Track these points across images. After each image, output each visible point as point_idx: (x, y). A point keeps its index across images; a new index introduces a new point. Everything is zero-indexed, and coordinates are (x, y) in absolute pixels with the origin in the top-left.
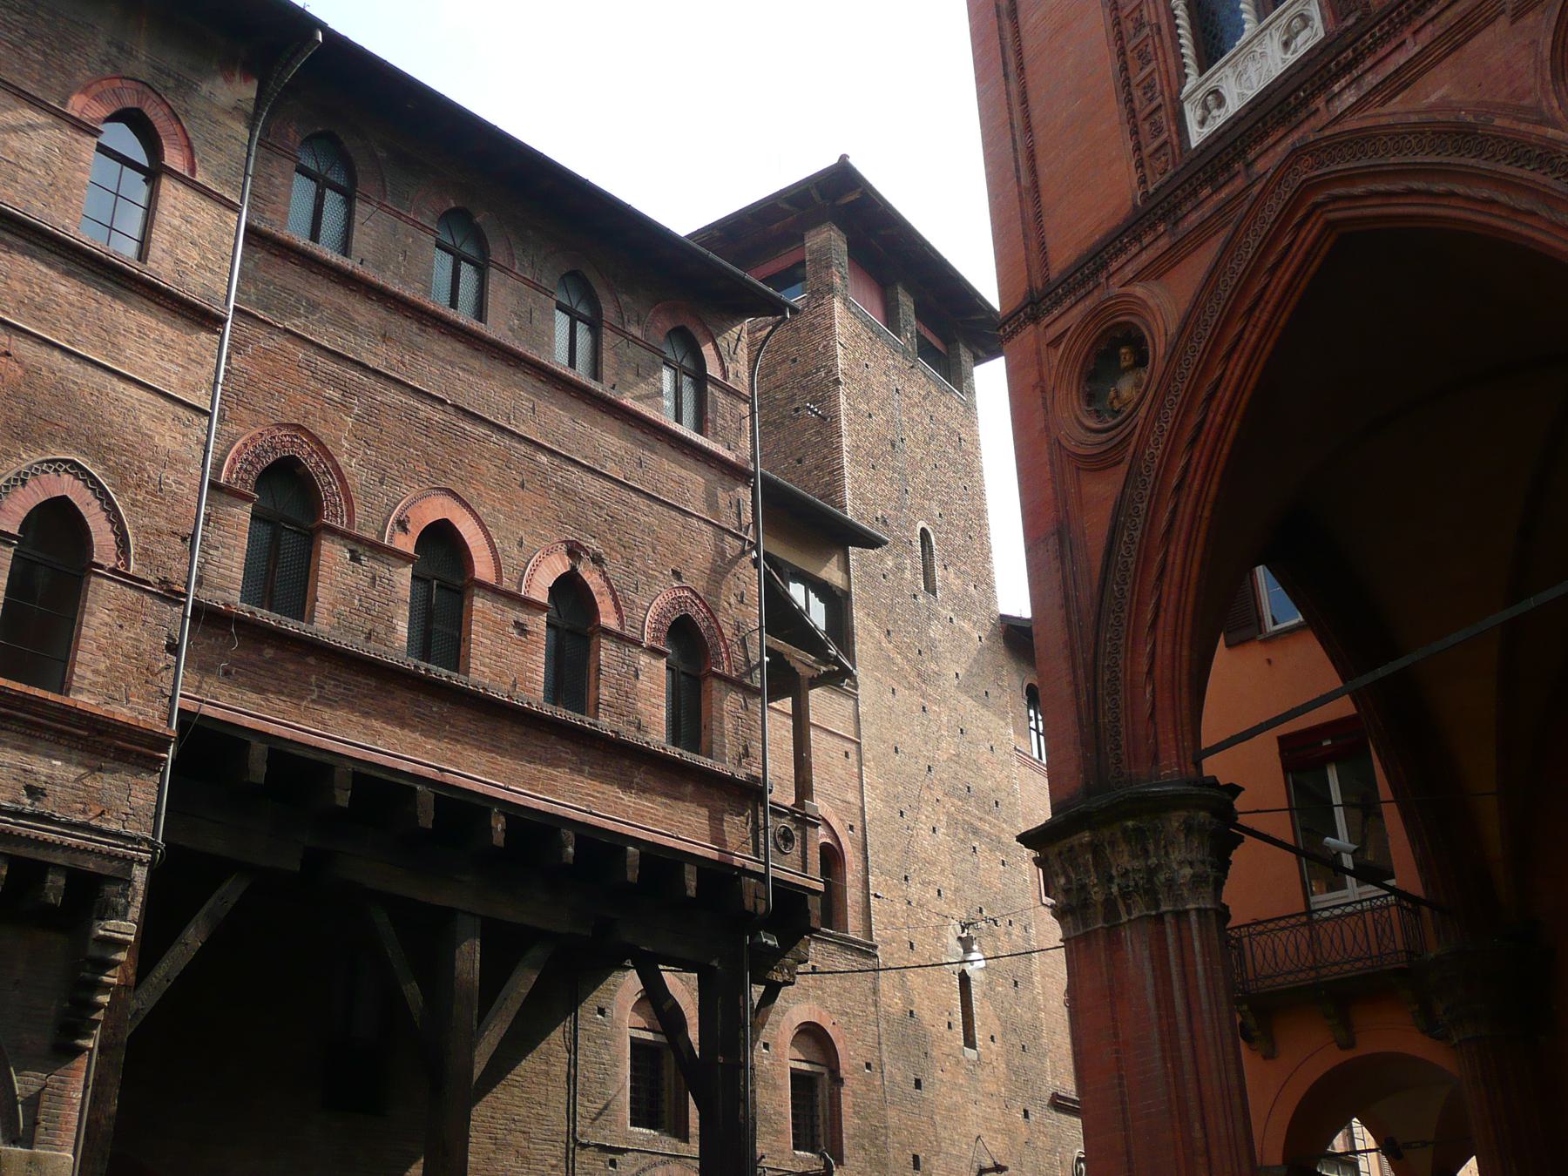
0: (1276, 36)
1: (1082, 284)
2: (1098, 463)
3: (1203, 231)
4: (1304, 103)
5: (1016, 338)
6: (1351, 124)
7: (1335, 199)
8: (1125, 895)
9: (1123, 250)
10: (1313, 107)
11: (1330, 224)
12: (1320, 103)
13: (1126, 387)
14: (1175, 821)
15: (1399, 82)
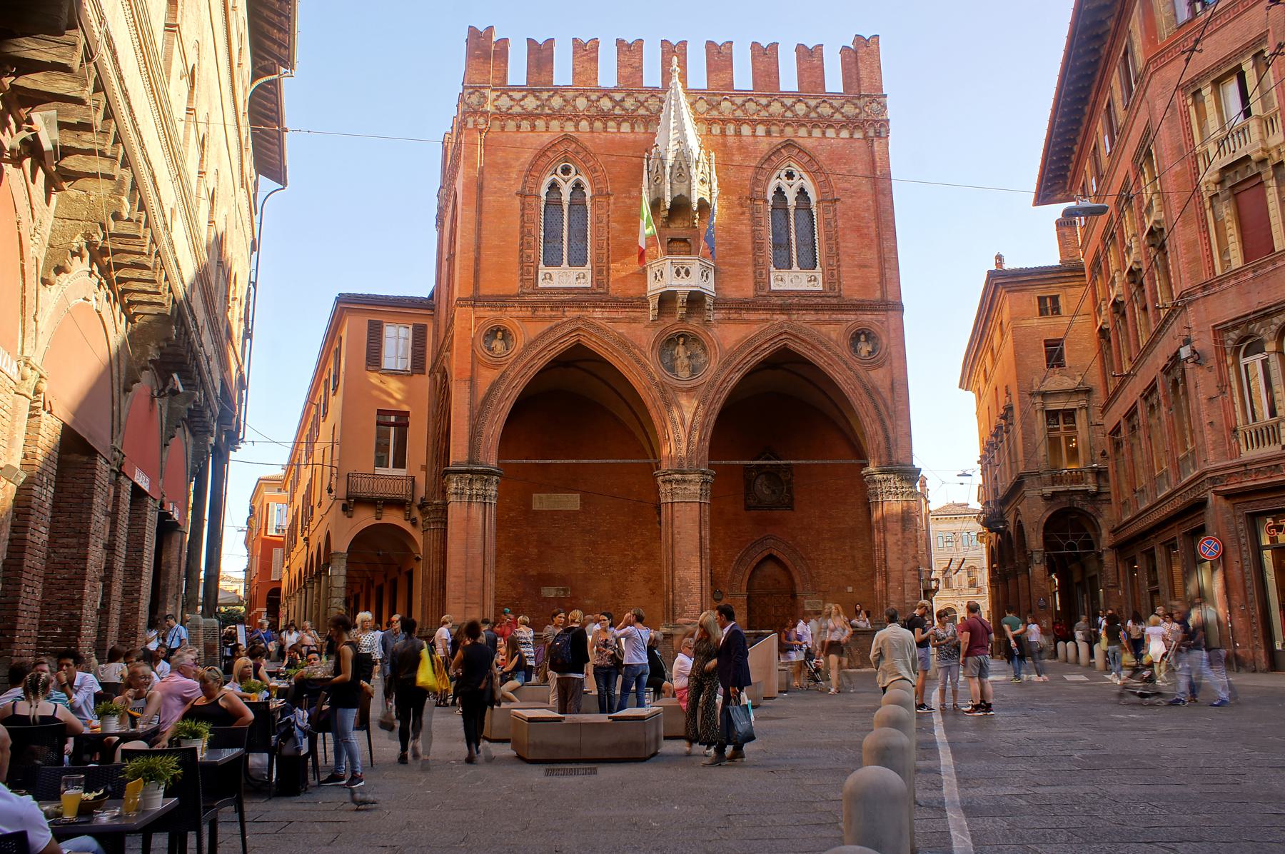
3: (543, 319)
6: (598, 322)
8: (477, 495)
10: (589, 309)
12: (591, 310)
13: (498, 345)
14: (495, 478)
15: (612, 320)
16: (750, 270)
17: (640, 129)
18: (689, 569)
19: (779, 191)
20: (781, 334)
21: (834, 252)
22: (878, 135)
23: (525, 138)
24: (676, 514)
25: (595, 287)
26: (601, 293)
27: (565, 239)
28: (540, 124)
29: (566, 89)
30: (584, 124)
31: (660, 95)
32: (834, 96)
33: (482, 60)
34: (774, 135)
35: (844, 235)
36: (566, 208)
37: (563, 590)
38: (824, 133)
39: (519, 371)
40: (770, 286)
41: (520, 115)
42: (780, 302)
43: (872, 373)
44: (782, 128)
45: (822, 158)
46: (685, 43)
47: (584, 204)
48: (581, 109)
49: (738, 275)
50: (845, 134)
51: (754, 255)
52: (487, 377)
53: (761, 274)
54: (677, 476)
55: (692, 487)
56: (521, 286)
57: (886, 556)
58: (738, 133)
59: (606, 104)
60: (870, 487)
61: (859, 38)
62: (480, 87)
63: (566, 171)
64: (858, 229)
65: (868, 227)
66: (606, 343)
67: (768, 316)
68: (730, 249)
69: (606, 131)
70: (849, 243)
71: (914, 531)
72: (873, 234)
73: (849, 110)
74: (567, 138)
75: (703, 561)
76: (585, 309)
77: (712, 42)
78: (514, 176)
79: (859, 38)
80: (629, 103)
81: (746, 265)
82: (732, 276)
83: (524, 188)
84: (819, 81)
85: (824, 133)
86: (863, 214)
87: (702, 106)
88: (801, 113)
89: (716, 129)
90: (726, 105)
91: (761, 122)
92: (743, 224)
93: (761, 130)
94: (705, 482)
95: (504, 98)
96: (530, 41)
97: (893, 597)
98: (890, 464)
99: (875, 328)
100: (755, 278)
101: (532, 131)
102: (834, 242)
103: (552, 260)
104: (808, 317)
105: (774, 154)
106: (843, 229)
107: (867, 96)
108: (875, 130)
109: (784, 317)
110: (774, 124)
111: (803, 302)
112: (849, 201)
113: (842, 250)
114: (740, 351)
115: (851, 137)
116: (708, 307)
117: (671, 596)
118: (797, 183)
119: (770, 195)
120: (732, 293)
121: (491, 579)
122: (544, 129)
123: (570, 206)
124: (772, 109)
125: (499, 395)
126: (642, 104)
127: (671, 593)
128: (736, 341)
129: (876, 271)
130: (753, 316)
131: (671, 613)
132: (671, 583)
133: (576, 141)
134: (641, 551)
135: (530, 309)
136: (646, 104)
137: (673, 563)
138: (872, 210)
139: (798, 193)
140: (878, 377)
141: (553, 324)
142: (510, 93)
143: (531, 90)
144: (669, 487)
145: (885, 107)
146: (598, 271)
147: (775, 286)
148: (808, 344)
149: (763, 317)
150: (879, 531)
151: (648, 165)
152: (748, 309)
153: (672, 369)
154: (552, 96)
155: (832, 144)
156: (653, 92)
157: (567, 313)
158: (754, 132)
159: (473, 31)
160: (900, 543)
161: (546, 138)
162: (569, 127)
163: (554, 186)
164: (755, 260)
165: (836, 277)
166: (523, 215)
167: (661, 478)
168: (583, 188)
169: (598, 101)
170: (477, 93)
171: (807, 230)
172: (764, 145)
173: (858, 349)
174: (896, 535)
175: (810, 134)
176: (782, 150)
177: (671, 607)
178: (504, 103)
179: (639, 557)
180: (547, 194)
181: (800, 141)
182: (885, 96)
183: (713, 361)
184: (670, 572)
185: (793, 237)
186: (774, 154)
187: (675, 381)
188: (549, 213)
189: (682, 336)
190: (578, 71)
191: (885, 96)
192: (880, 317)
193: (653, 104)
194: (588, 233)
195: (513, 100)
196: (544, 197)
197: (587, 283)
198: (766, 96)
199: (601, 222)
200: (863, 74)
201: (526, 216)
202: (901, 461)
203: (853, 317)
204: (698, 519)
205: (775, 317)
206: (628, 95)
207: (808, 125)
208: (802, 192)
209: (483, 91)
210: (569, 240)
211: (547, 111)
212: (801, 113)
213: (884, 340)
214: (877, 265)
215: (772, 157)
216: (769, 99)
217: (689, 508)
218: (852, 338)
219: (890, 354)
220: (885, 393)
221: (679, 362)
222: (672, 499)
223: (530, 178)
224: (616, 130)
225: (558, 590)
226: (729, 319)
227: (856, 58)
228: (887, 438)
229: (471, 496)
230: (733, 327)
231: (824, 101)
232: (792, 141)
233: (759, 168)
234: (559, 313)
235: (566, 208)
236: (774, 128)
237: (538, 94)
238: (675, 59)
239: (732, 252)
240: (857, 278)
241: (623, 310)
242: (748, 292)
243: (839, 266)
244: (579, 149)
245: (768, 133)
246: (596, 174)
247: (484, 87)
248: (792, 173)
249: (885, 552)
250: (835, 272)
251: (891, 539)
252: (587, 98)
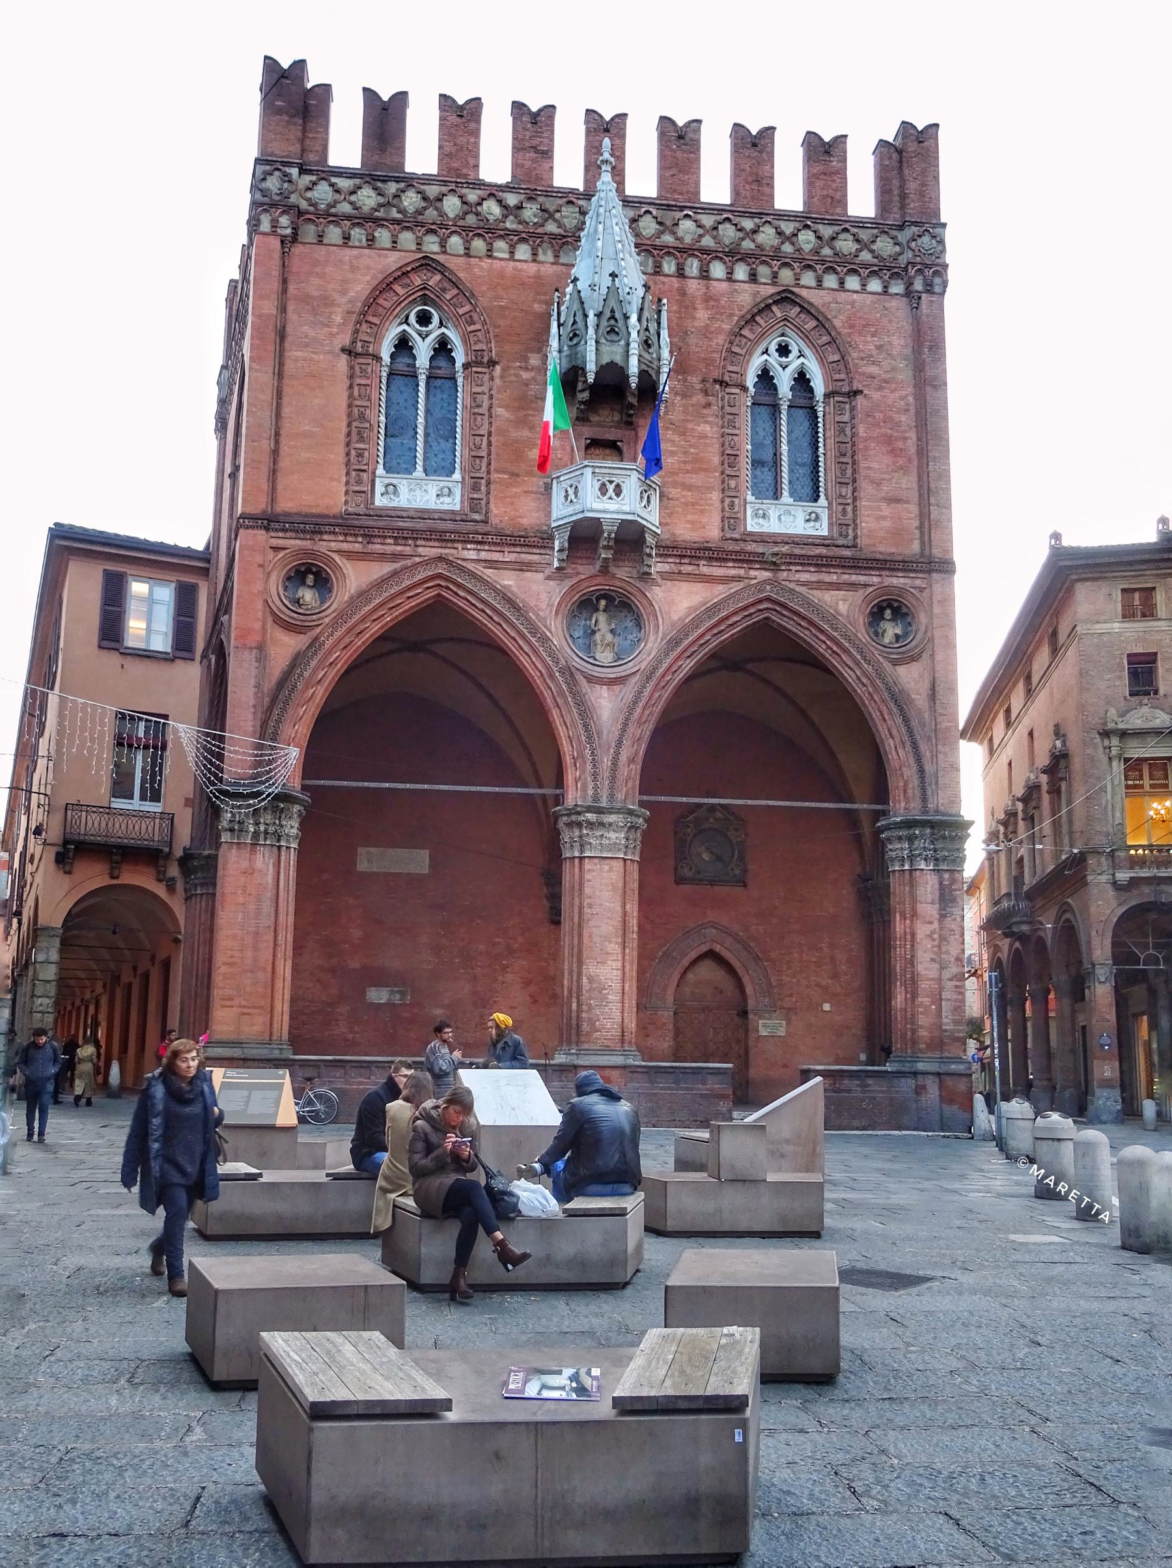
0: (435, 488)
1: (304, 532)
2: (290, 627)
3: (382, 557)
4: (453, 541)
5: (250, 531)
6: (470, 566)
7: (447, 588)
8: (266, 832)
9: (334, 533)
10: (456, 545)
11: (439, 595)
12: (459, 546)
14: (296, 808)
15: (491, 564)
16: (715, 496)
17: (546, 256)
18: (603, 963)
19: (766, 378)
20: (760, 601)
21: (849, 478)
22: (929, 288)
23: (357, 257)
24: (587, 876)
25: (467, 510)
26: (476, 521)
27: (420, 431)
28: (383, 236)
29: (427, 179)
30: (455, 242)
31: (581, 202)
32: (860, 223)
33: (286, 118)
34: (763, 280)
35: (866, 449)
36: (422, 379)
37: (398, 992)
38: (842, 283)
39: (341, 639)
40: (745, 525)
41: (348, 217)
42: (761, 550)
43: (902, 670)
44: (776, 269)
45: (837, 323)
46: (623, 116)
47: (453, 379)
48: (451, 215)
49: (697, 503)
50: (875, 285)
51: (723, 473)
52: (285, 645)
53: (732, 505)
54: (589, 816)
55: (613, 835)
56: (346, 502)
57: (913, 956)
58: (705, 275)
59: (492, 209)
60: (890, 847)
61: (906, 126)
62: (285, 164)
63: (424, 319)
64: (889, 440)
65: (906, 439)
66: (482, 601)
67: (742, 572)
68: (685, 462)
69: (490, 256)
70: (874, 462)
71: (959, 919)
72: (913, 450)
73: (885, 246)
74: (427, 263)
75: (627, 951)
76: (449, 545)
77: (669, 119)
78: (338, 319)
79: (906, 126)
80: (530, 212)
81: (710, 489)
82: (686, 504)
83: (354, 342)
84: (838, 196)
85: (842, 283)
86: (896, 417)
87: (648, 226)
88: (807, 248)
89: (669, 266)
90: (687, 226)
91: (744, 258)
92: (707, 422)
93: (741, 272)
94: (633, 828)
95: (323, 187)
96: (370, 95)
97: (923, 1020)
98: (925, 811)
99: (908, 601)
100: (723, 510)
101: (369, 247)
102: (850, 461)
103: (400, 464)
104: (805, 577)
105: (760, 312)
106: (866, 440)
107: (915, 223)
108: (925, 279)
109: (767, 575)
110: (763, 262)
111: (797, 551)
112: (876, 395)
113: (863, 472)
114: (696, 622)
115: (885, 292)
116: (648, 550)
117: (574, 1005)
118: (794, 363)
119: (751, 380)
120: (685, 532)
121: (285, 969)
122: (389, 245)
123: (429, 378)
124: (760, 238)
125: (306, 674)
126: (551, 216)
127: (574, 1000)
128: (689, 608)
129: (914, 509)
130: (718, 571)
131: (574, 1032)
132: (575, 983)
133: (440, 268)
134: (520, 939)
135: (360, 539)
136: (557, 215)
137: (580, 952)
138: (913, 411)
139: (795, 379)
140: (910, 677)
141: (397, 566)
142: (334, 180)
143: (369, 176)
144: (577, 833)
145: (941, 242)
146: (473, 484)
147: (753, 525)
148: (804, 618)
149: (733, 572)
150: (904, 917)
151: (559, 314)
152: (710, 559)
153: (589, 648)
154: (403, 191)
155: (854, 301)
156: (569, 196)
157: (420, 550)
158: (731, 273)
159: (270, 64)
160: (936, 936)
161: (393, 261)
162: (432, 245)
163: (403, 345)
164: (723, 482)
165: (850, 515)
166: (351, 387)
167: (565, 819)
168: (451, 350)
169: (480, 204)
170: (277, 173)
171: (805, 442)
172: (746, 296)
173: (880, 631)
174: (931, 923)
175: (819, 281)
176: (774, 308)
177: (574, 1022)
178: (323, 196)
179: (516, 946)
180: (392, 356)
181: (804, 293)
182: (944, 225)
183: (652, 638)
184: (575, 966)
185: (784, 448)
186: (760, 312)
187: (590, 667)
188: (393, 387)
189: (604, 596)
190: (447, 150)
191: (944, 225)
192: (918, 582)
193: (569, 216)
194: (459, 423)
195: (337, 191)
196: (386, 359)
197: (454, 503)
198: (752, 215)
199: (479, 406)
200: (912, 186)
201: (356, 389)
202: (942, 808)
203: (875, 579)
204: (621, 884)
205: (753, 573)
206: (530, 199)
207: (817, 267)
208: (802, 380)
209: (287, 170)
210: (427, 435)
211: (394, 214)
212: (807, 248)
213: (923, 618)
214: (916, 500)
215: (758, 318)
216: (757, 220)
217: (606, 868)
218: (872, 614)
219: (931, 640)
220: (920, 699)
221: (598, 637)
222: (582, 851)
223: (364, 326)
224: (506, 256)
225: (392, 992)
226: (680, 573)
227: (901, 162)
228: (921, 771)
229: (256, 834)
230: (685, 587)
231: (846, 230)
232: (792, 293)
233: (737, 334)
234: (408, 548)
235: (422, 379)
236: (764, 271)
237: (379, 184)
238: (607, 142)
239: (688, 467)
240: (884, 518)
241: (512, 549)
242: (712, 531)
243: (855, 499)
244: (446, 285)
245: (753, 277)
246: (472, 328)
247: (289, 164)
248: (787, 346)
249: (913, 946)
250: (849, 509)
251: (922, 930)
252: (461, 197)
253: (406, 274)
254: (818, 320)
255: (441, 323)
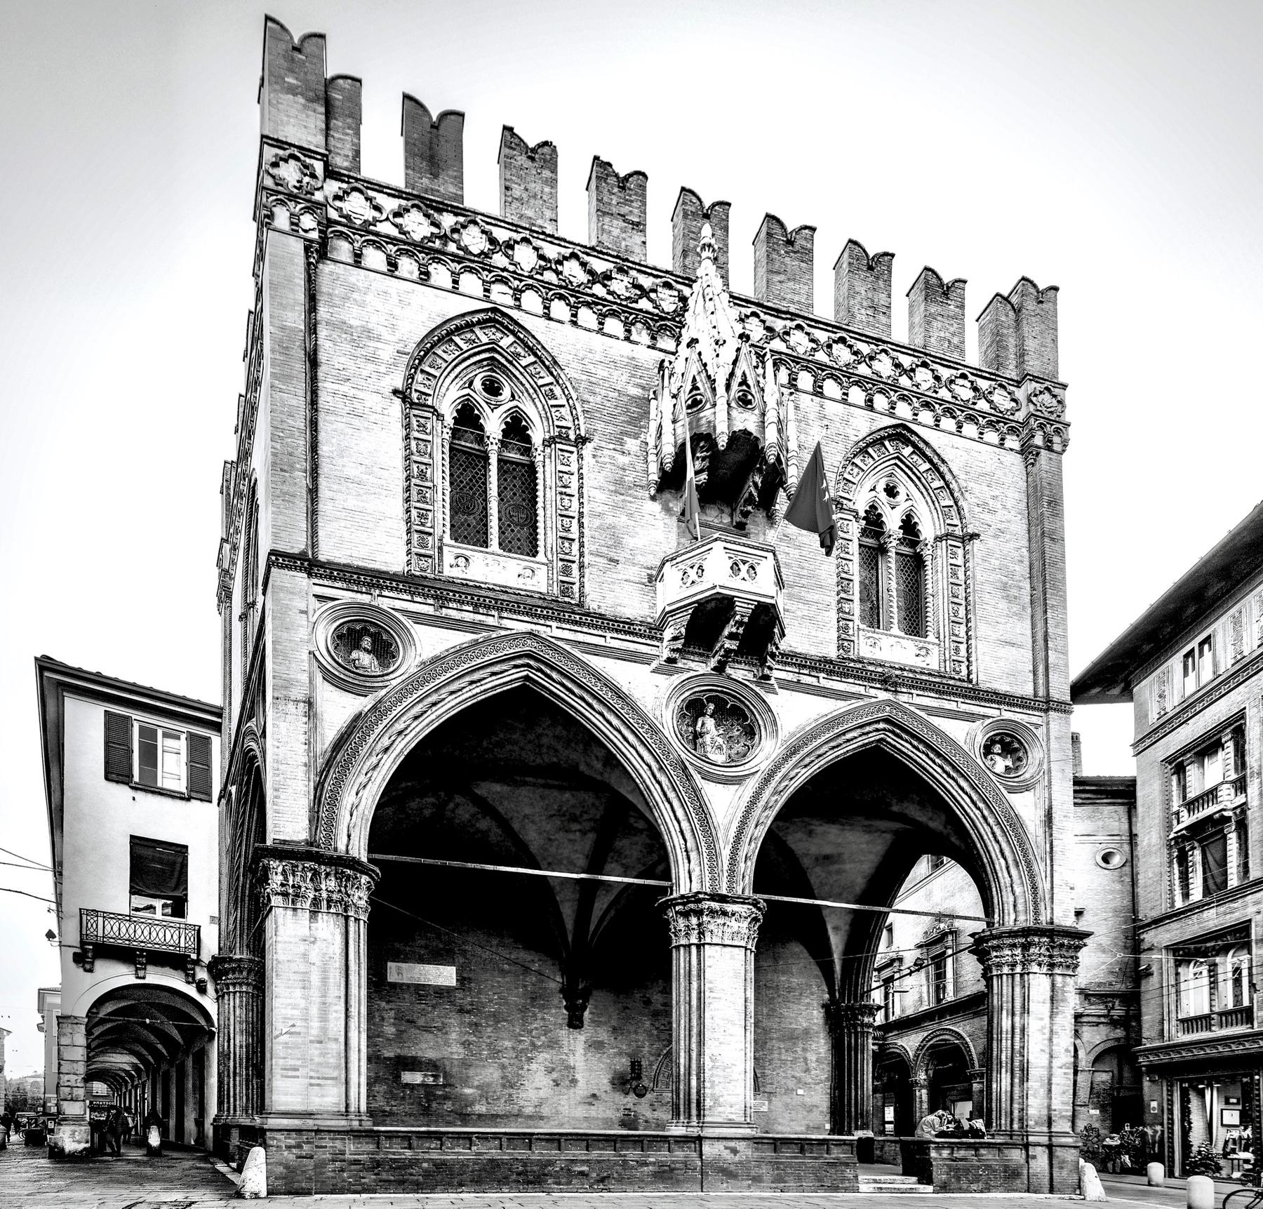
44: (894, 399)
216: (873, 346)
253: (470, 326)
254: (931, 462)
255: (513, 396)
